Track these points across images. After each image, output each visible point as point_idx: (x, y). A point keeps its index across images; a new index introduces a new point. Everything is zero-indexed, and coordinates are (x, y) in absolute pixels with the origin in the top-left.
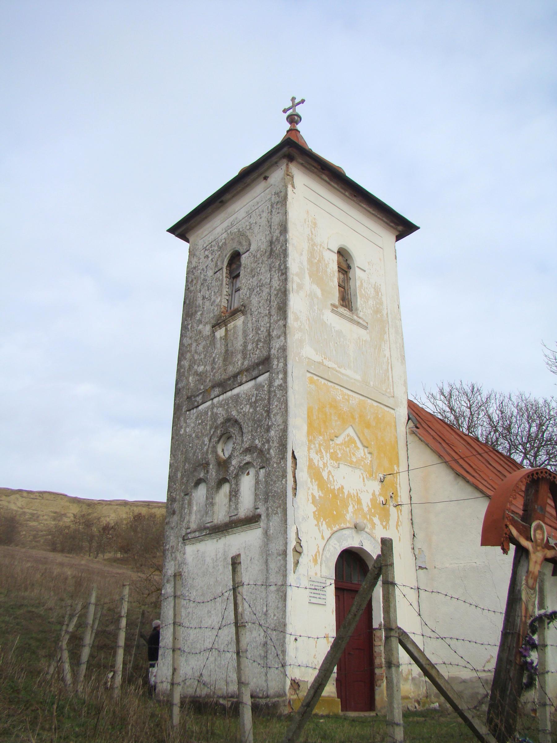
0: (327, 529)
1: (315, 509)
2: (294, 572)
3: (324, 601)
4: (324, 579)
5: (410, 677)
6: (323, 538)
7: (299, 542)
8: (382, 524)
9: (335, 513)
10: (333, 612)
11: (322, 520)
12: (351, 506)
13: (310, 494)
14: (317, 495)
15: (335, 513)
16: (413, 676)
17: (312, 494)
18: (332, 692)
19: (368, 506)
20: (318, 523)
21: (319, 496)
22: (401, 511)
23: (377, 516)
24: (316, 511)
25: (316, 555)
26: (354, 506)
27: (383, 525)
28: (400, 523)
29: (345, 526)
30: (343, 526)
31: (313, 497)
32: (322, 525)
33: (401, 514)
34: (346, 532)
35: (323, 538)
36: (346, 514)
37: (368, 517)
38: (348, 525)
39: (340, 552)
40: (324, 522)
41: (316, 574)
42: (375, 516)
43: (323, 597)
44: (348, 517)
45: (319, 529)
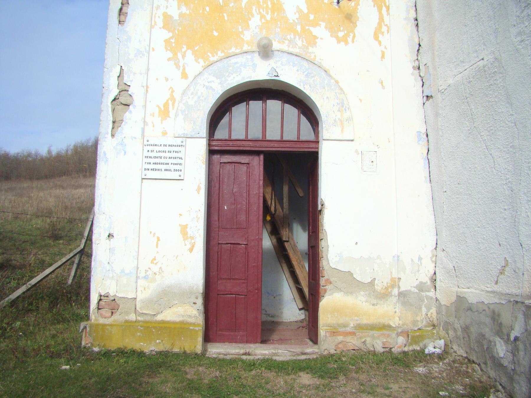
0: (196, 60)
1: (171, 35)
2: (113, 136)
3: (179, 173)
4: (181, 139)
5: (395, 291)
6: (184, 76)
7: (124, 89)
8: (334, 34)
9: (216, 34)
10: (198, 190)
11: (184, 50)
12: (257, 17)
13: (160, 13)
14: (174, 12)
15: (216, 34)
16: (402, 289)
17: (165, 15)
18: (190, 316)
19: (299, 10)
20: (175, 54)
21: (181, 15)
22: (388, 8)
23: (323, 24)
24: (171, 38)
25: (166, 105)
26: (262, 17)
27: (337, 37)
28: (384, 29)
29: (238, 51)
30: (233, 50)
31: (167, 18)
32: (184, 56)
33: (388, 14)
34: (240, 59)
35: (184, 76)
36: (242, 33)
37: (299, 28)
38: (246, 48)
39: (221, 93)
40: (189, 52)
41: (165, 133)
42: (315, 24)
43: (178, 167)
44: (247, 36)
45: (177, 66)
